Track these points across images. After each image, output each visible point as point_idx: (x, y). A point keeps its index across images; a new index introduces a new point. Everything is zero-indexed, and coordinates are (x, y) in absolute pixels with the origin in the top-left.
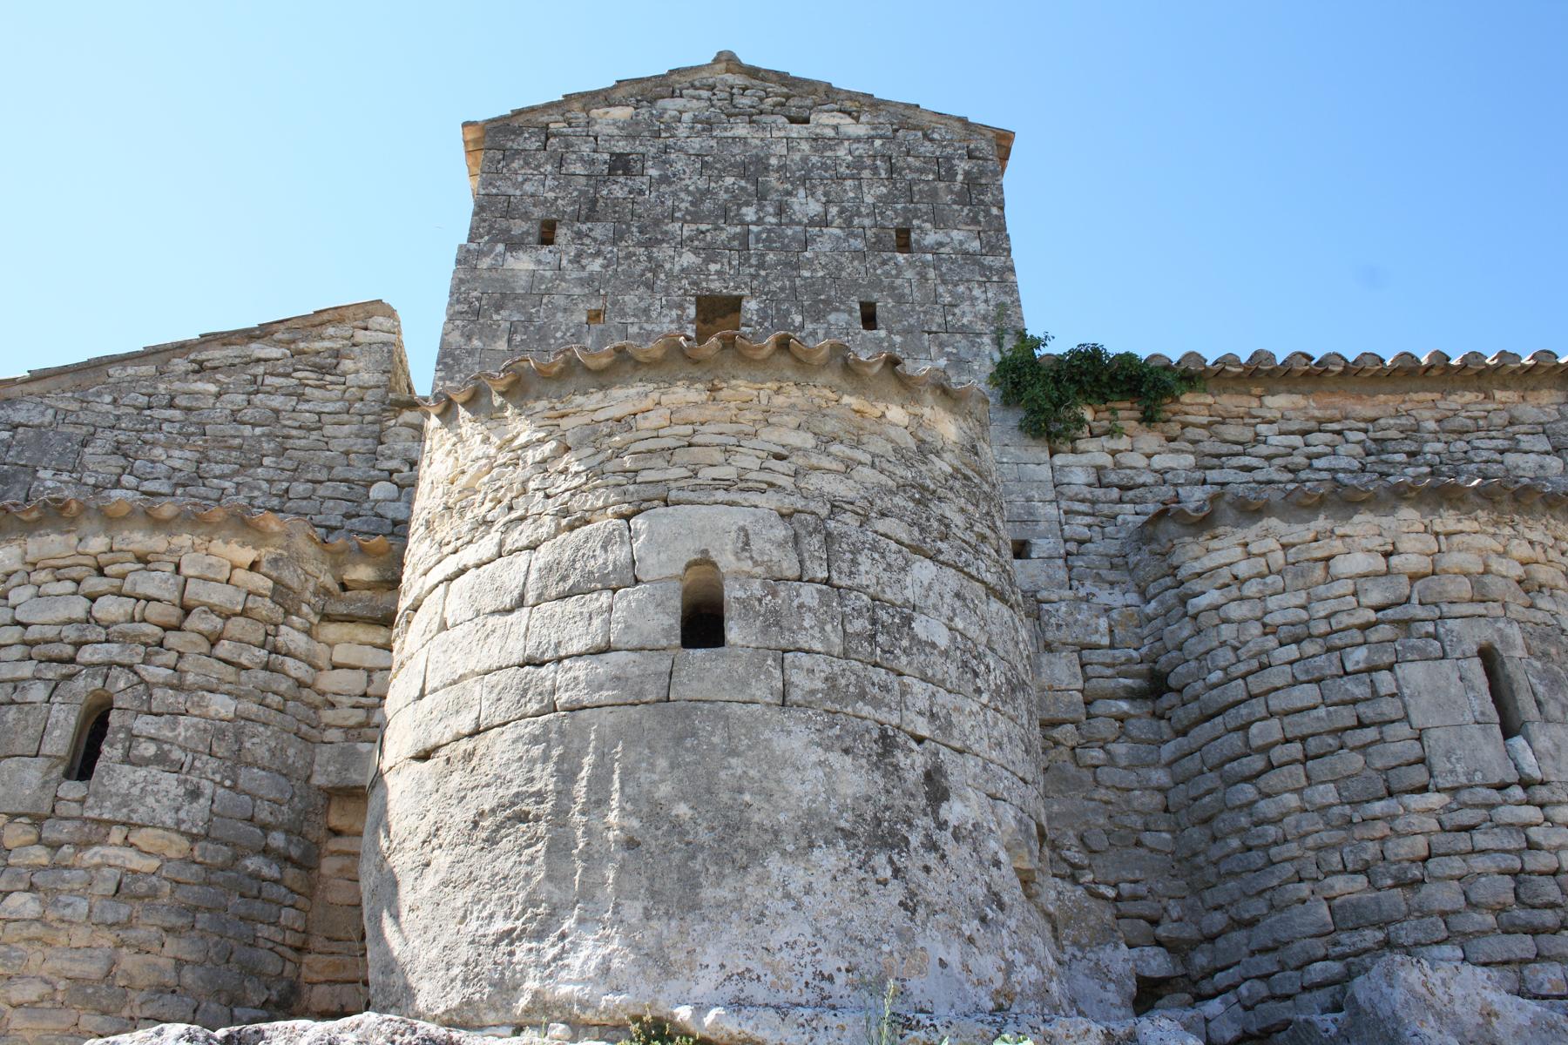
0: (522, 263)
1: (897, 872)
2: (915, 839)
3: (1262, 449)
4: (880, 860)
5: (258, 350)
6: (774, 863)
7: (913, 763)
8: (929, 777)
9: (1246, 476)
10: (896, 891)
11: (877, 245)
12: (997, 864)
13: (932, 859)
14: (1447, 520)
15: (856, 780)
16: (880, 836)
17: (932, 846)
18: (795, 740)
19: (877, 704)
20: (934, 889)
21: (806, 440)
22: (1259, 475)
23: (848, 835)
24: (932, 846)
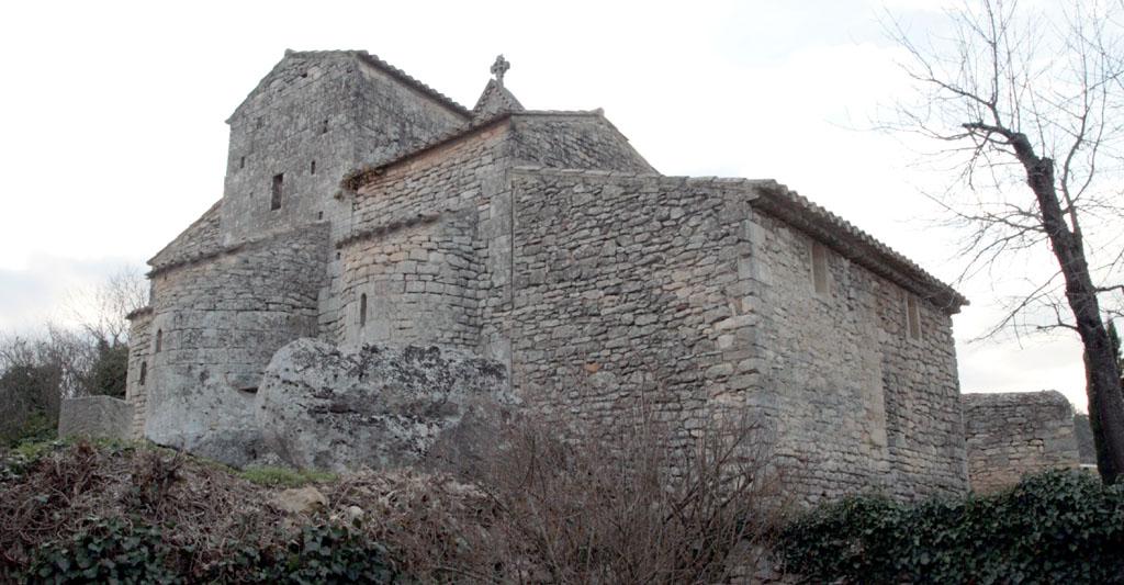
0: (237, 179)
1: (187, 401)
2: (194, 391)
3: (406, 192)
4: (183, 399)
5: (203, 225)
6: (163, 403)
7: (197, 371)
8: (202, 374)
9: (399, 205)
10: (186, 405)
11: (319, 134)
12: (223, 391)
13: (198, 395)
14: (367, 244)
15: (181, 380)
16: (186, 392)
17: (199, 392)
18: (169, 373)
19: (188, 359)
20: (197, 404)
21: (179, 288)
22: (403, 204)
23: (177, 394)
24: (199, 392)
